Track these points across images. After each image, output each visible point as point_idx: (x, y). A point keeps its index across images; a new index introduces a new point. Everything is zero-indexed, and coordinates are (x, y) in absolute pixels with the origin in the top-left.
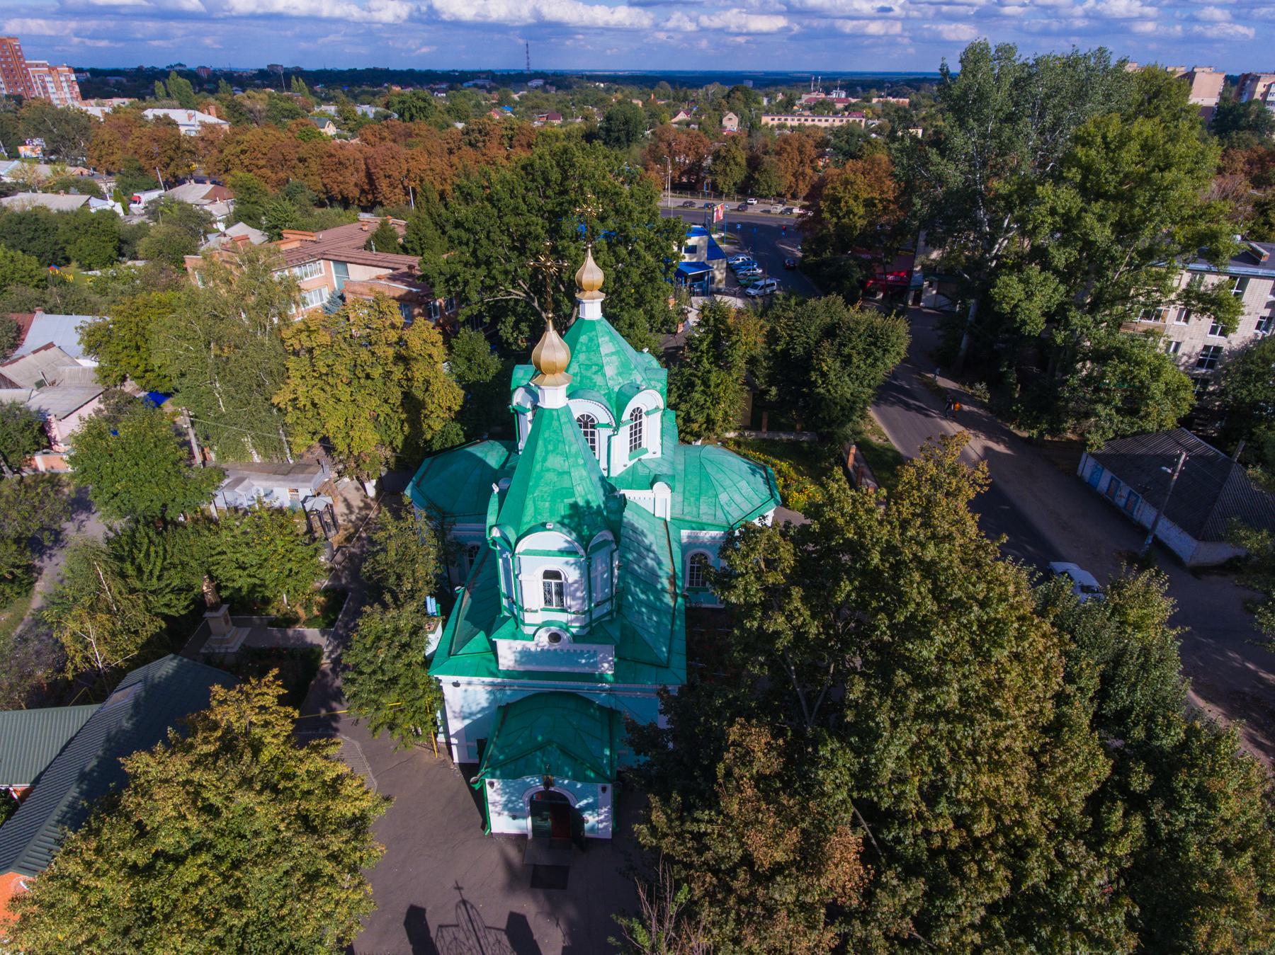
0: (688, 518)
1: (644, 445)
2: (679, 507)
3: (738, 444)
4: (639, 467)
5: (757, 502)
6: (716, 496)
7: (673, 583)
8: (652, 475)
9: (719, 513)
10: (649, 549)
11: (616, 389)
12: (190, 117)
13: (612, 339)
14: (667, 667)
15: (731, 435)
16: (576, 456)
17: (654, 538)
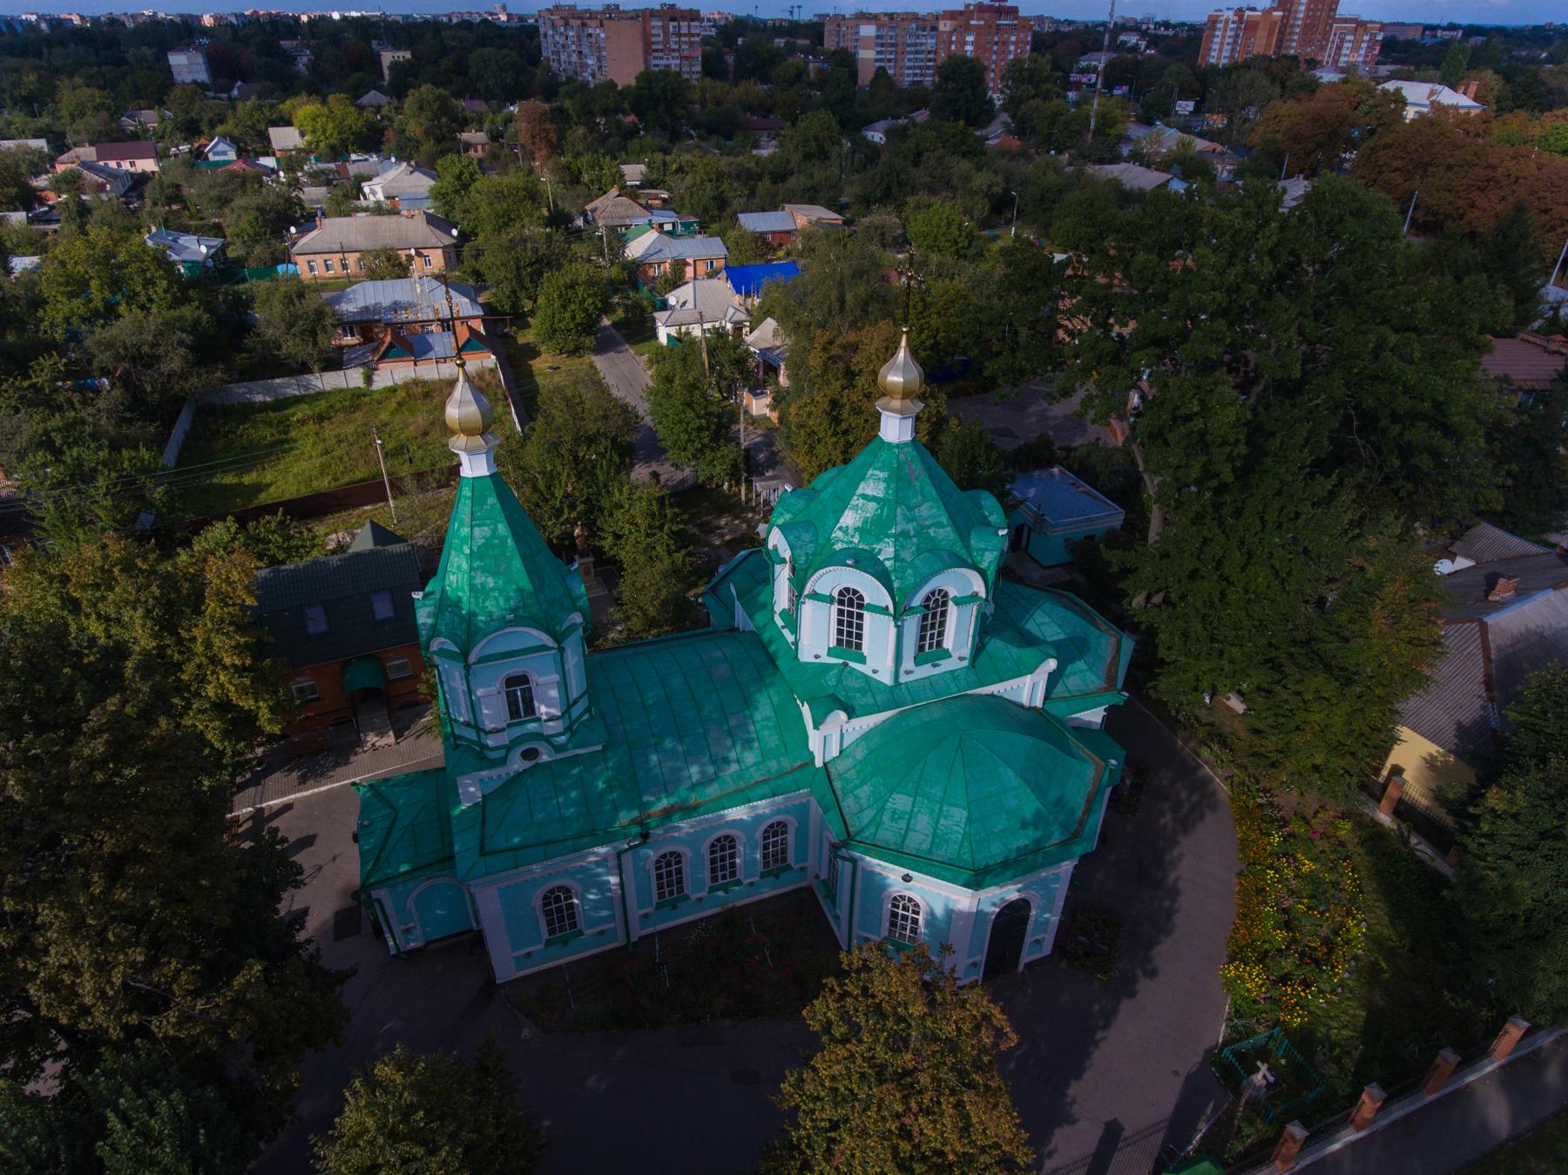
0: (837, 784)
1: (865, 650)
2: (849, 763)
3: (1374, 836)
4: (835, 671)
5: (942, 853)
6: (892, 791)
7: (667, 813)
8: (830, 691)
9: (869, 814)
10: (721, 762)
11: (838, 546)
12: (1432, 93)
13: (899, 479)
14: (483, 852)
15: (1385, 818)
16: (463, 540)
17: (746, 761)
